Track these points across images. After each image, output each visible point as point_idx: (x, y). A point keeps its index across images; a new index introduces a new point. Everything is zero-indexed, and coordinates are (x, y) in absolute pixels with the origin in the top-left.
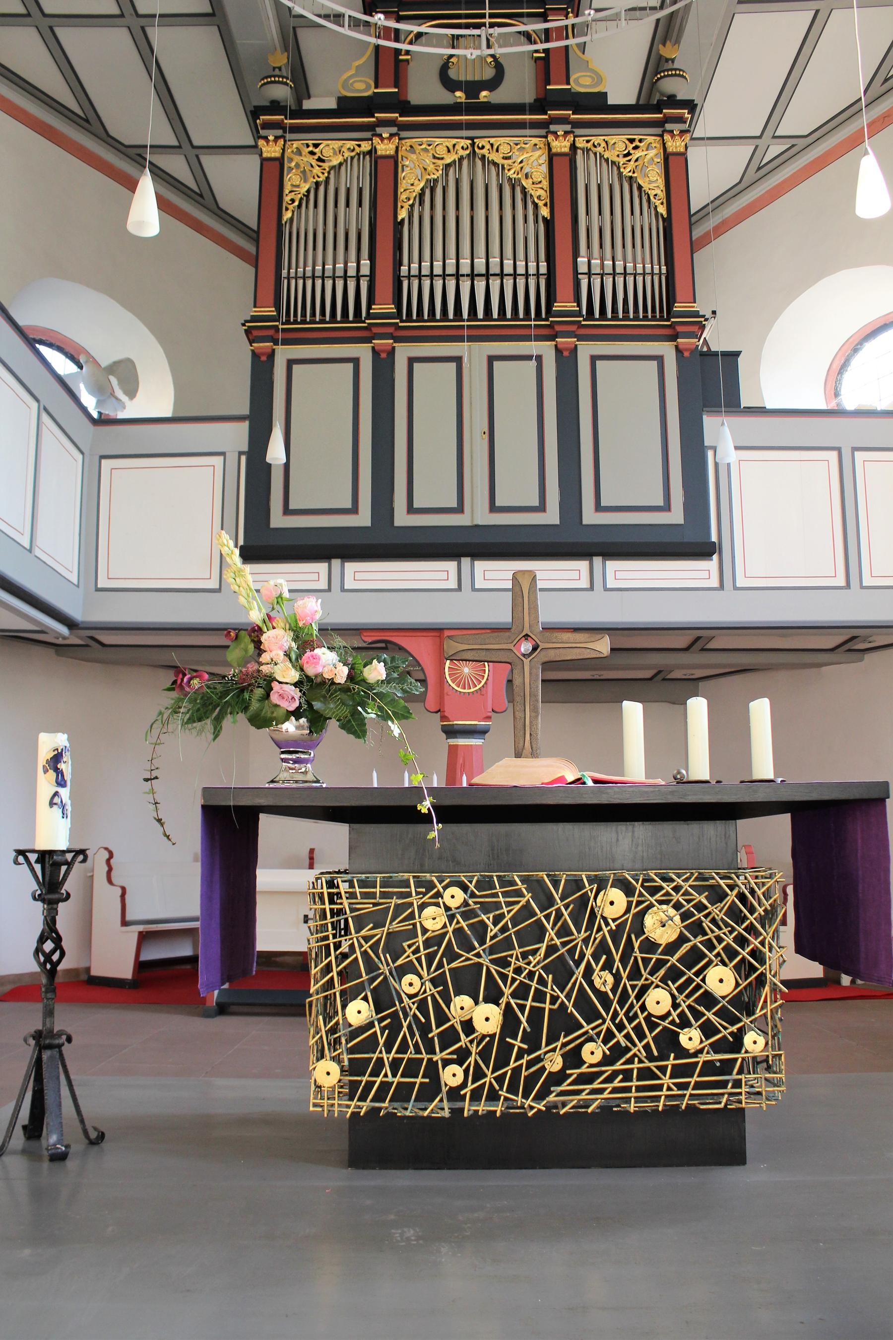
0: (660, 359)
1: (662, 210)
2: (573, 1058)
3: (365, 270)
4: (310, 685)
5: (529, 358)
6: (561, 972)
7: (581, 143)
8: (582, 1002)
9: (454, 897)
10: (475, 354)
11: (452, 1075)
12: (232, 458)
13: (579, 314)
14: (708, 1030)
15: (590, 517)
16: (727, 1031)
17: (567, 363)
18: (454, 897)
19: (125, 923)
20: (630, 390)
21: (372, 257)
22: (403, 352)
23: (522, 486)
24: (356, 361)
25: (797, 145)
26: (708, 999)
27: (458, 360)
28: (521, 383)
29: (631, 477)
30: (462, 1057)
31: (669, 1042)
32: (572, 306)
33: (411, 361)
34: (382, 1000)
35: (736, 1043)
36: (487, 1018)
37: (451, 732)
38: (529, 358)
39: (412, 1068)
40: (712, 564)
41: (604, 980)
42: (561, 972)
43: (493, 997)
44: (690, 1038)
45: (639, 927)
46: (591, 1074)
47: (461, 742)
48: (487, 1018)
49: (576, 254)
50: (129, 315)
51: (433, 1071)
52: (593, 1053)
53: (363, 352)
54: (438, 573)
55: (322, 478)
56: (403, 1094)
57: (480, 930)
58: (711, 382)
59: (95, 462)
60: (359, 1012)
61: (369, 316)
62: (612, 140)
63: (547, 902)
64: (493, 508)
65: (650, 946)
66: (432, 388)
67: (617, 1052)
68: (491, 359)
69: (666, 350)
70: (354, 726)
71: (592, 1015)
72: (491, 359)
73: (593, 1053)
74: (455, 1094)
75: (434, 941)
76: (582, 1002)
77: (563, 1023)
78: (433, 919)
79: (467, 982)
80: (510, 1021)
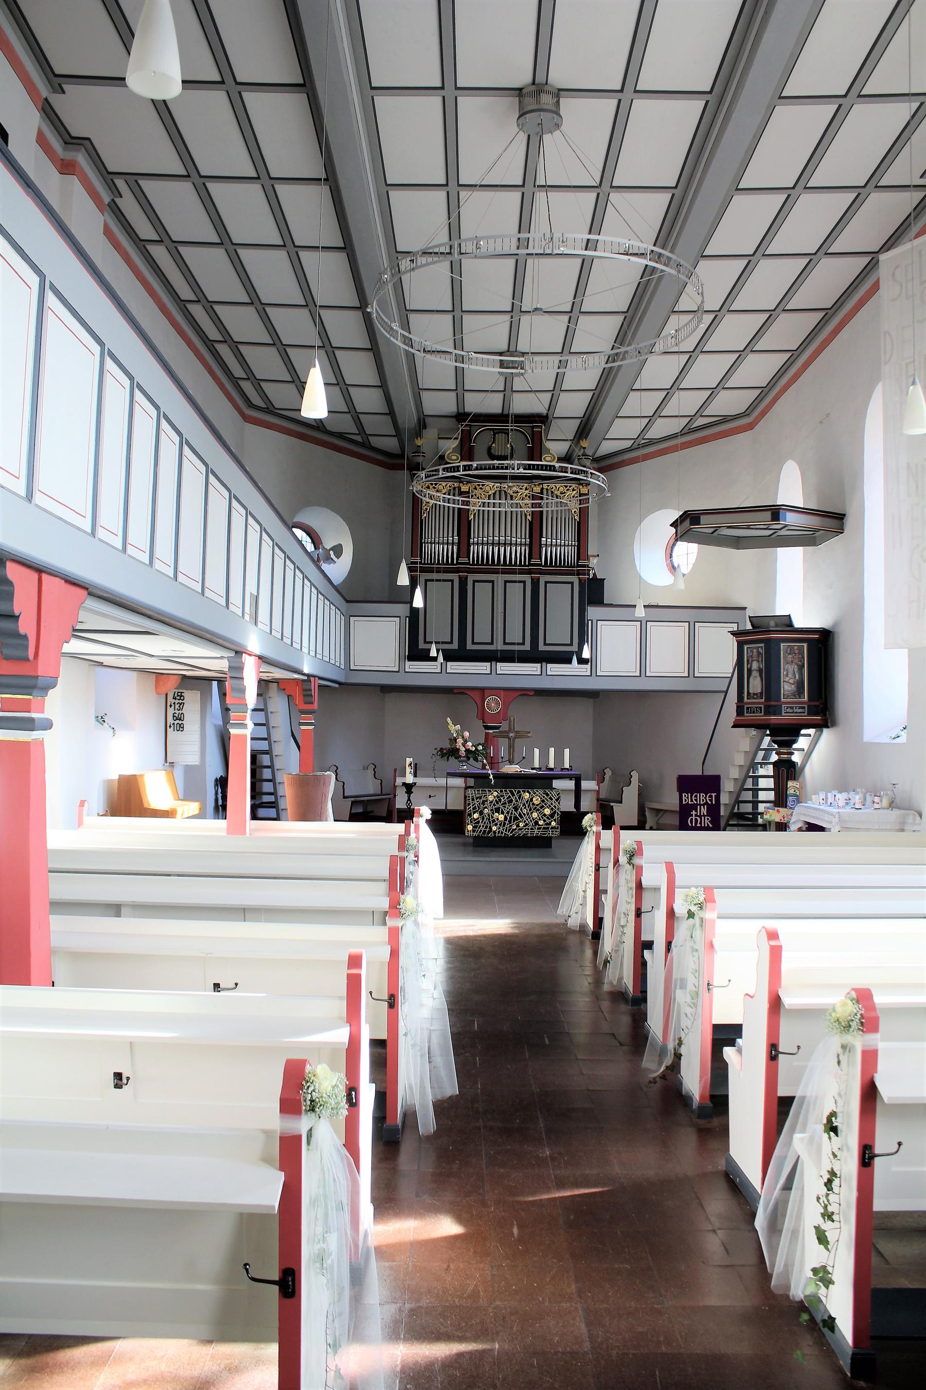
0: (572, 583)
1: (577, 518)
2: (518, 826)
3: (456, 541)
4: (468, 751)
5: (520, 582)
6: (516, 809)
7: (545, 486)
8: (520, 815)
9: (495, 794)
10: (500, 579)
11: (494, 828)
12: (403, 618)
13: (541, 565)
14: (544, 821)
15: (542, 647)
16: (548, 821)
17: (535, 584)
18: (495, 794)
19: (344, 797)
20: (560, 598)
21: (459, 535)
22: (471, 578)
23: (516, 633)
24: (452, 581)
25: (652, 442)
26: (545, 815)
27: (492, 582)
28: (517, 595)
29: (558, 632)
30: (496, 825)
31: (536, 823)
32: (537, 561)
33: (474, 582)
34: (481, 813)
35: (550, 824)
36: (501, 817)
37: (487, 728)
38: (520, 582)
39: (486, 827)
40: (589, 666)
41: (525, 811)
42: (516, 809)
43: (503, 813)
44: (541, 822)
45: (532, 800)
46: (521, 828)
47: (491, 731)
48: (501, 817)
49: (541, 536)
50: (333, 514)
51: (490, 828)
52: (521, 825)
53: (455, 577)
54: (483, 667)
55: (439, 629)
56: (485, 832)
57: (500, 800)
58: (593, 592)
59: (348, 617)
60: (476, 816)
61: (458, 563)
62: (558, 486)
63: (513, 795)
64: (505, 643)
65: (533, 804)
66: (483, 591)
67: (527, 825)
68: (506, 582)
69: (575, 579)
70: (476, 760)
71: (522, 817)
72: (506, 582)
73: (521, 825)
74: (495, 832)
75: (491, 802)
76: (520, 815)
77: (516, 819)
78: (491, 798)
79: (497, 810)
80: (506, 818)
